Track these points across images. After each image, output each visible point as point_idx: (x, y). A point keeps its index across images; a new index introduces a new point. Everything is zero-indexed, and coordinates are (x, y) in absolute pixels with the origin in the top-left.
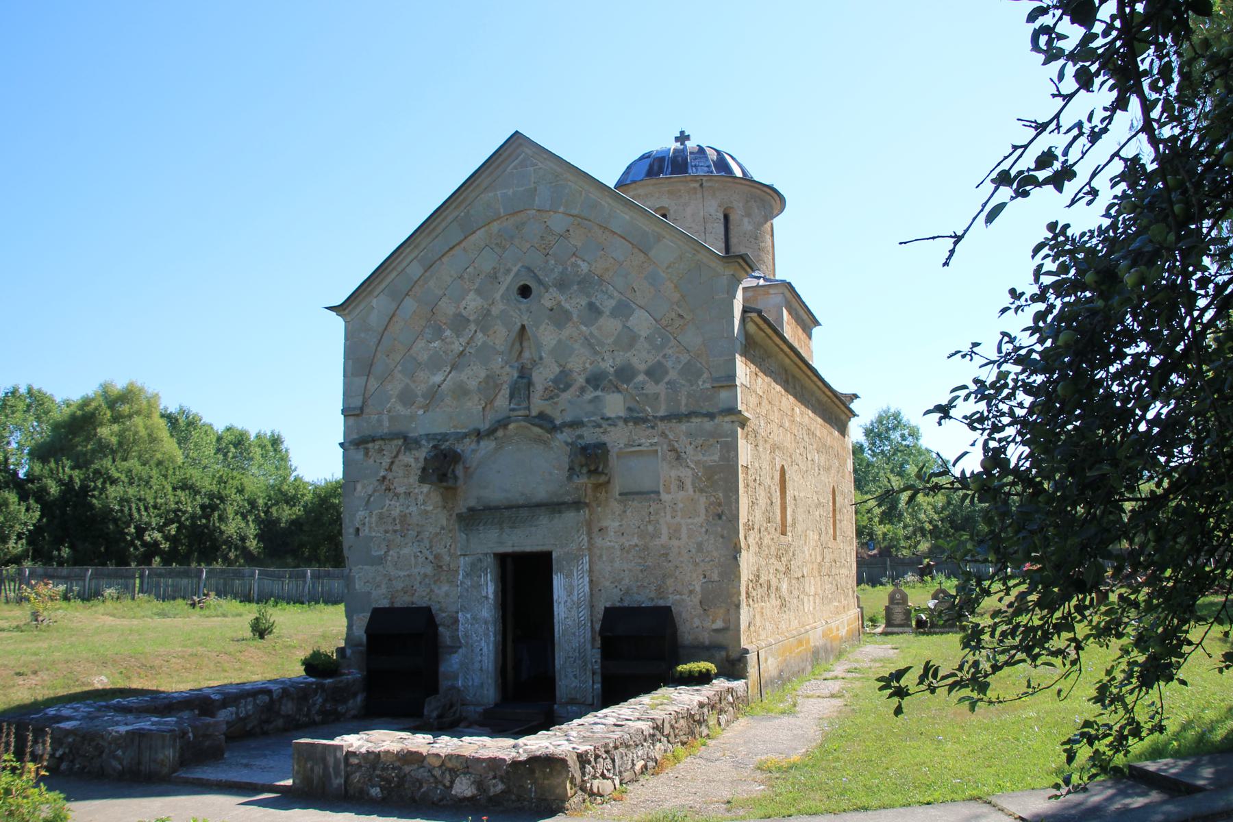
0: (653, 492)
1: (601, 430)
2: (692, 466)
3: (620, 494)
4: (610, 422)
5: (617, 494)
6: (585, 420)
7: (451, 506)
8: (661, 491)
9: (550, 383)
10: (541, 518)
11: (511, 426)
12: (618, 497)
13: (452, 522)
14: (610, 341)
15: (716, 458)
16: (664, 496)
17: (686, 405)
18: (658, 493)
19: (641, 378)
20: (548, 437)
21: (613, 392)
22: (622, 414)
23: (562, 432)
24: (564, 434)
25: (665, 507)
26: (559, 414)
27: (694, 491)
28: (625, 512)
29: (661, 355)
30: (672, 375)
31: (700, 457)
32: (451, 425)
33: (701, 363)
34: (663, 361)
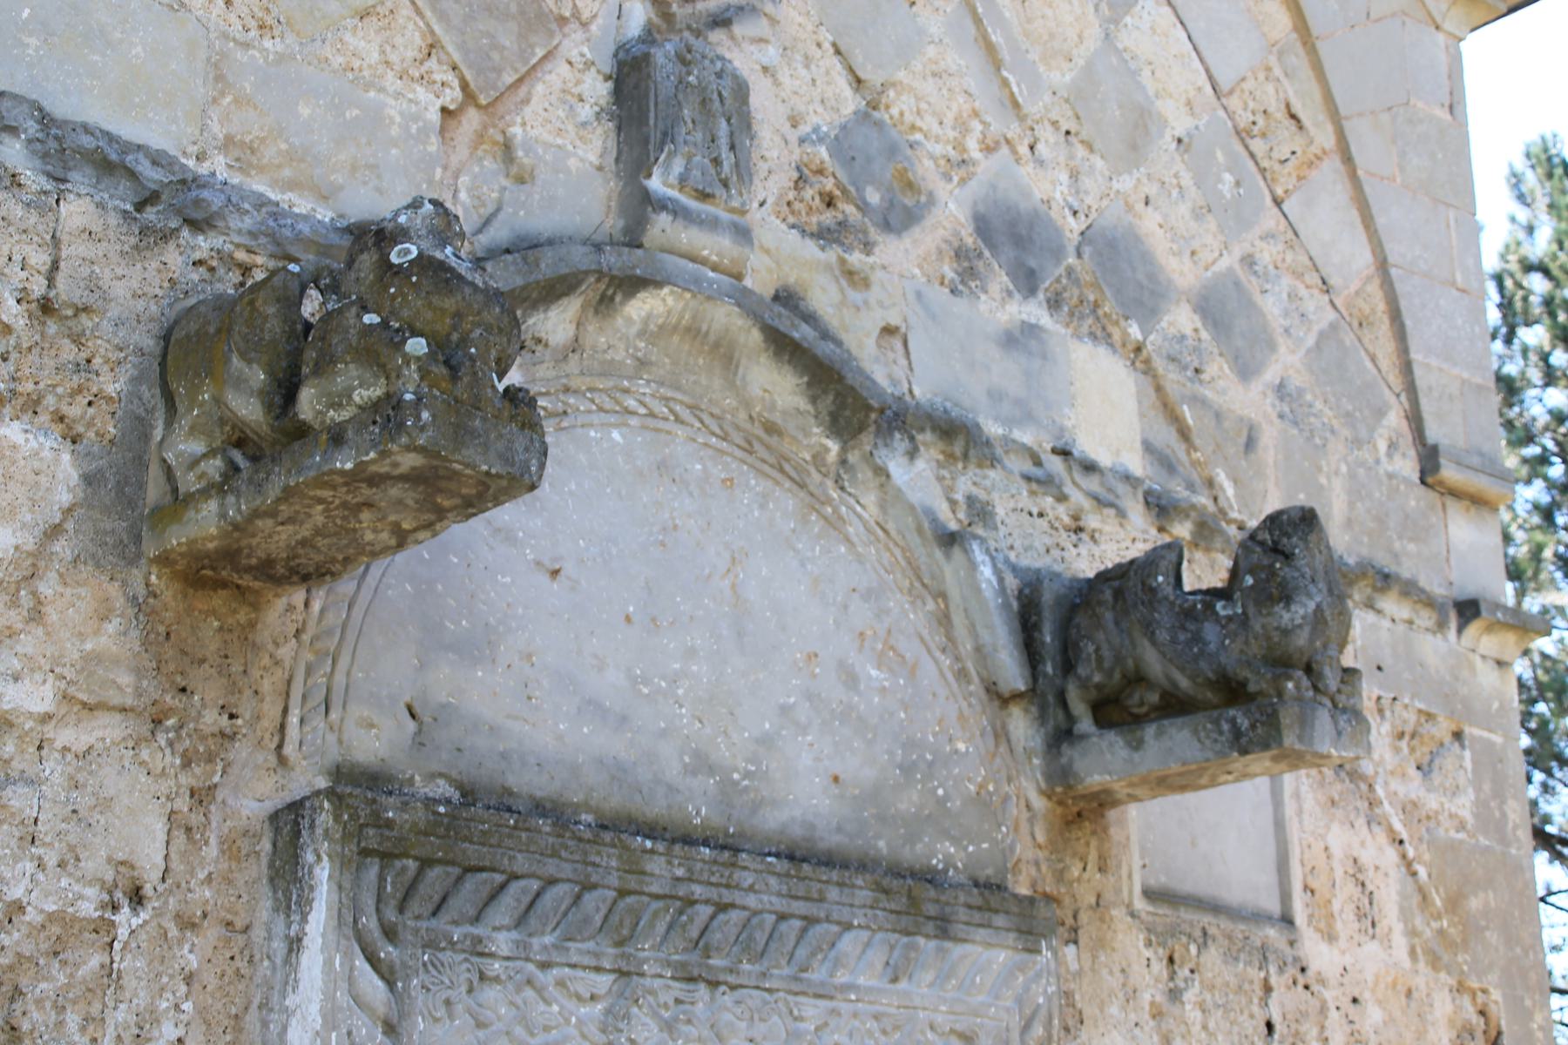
0: (1258, 917)
1: (1062, 512)
2: (1398, 826)
3: (1150, 894)
4: (1092, 483)
5: (1137, 889)
6: (993, 429)
7: (212, 719)
8: (1300, 918)
9: (823, 152)
10: (848, 943)
11: (642, 307)
12: (1140, 904)
13: (212, 851)
14: (1061, 76)
15: (1464, 805)
16: (1320, 955)
17: (1349, 523)
18: (1287, 920)
19: (1182, 319)
20: (818, 458)
21: (1093, 336)
22: (1136, 464)
23: (912, 454)
24: (921, 464)
25: (1323, 1010)
26: (871, 342)
27: (1412, 953)
28: (1175, 995)
29: (1237, 252)
30: (1287, 362)
31: (1413, 787)
32: (217, 129)
33: (1373, 359)
34: (1252, 284)
